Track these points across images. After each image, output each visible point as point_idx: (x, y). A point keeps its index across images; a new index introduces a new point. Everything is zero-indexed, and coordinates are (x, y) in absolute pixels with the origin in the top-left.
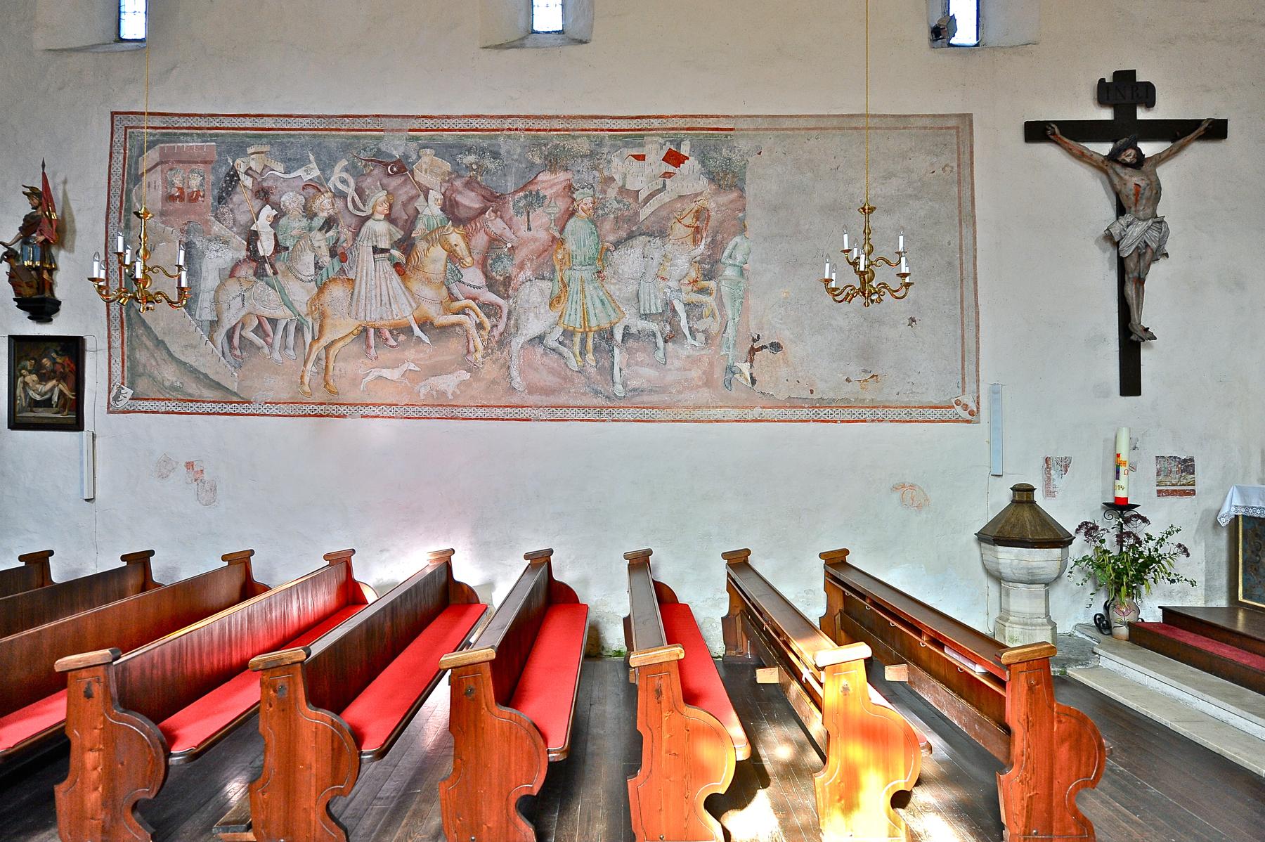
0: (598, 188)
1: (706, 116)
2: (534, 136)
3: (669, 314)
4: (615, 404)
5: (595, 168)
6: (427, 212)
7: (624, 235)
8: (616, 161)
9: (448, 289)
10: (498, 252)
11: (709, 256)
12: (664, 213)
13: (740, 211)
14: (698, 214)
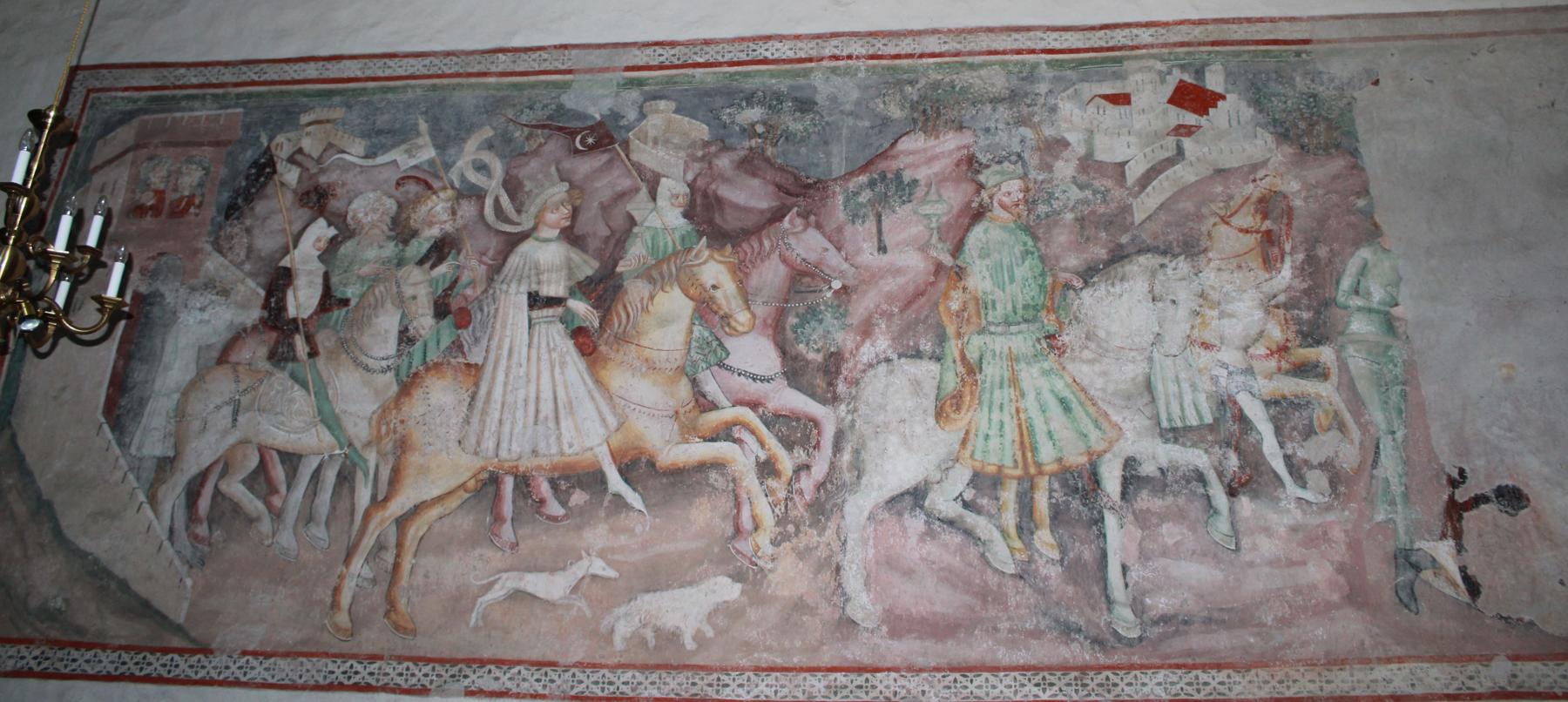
0: (1033, 160)
1: (1249, 20)
2: (888, 68)
3: (1229, 425)
4: (1116, 659)
5: (1022, 121)
6: (653, 221)
7: (1102, 253)
8: (1067, 107)
9: (694, 382)
10: (811, 299)
11: (1307, 292)
12: (1188, 205)
13: (1359, 195)
14: (1265, 205)
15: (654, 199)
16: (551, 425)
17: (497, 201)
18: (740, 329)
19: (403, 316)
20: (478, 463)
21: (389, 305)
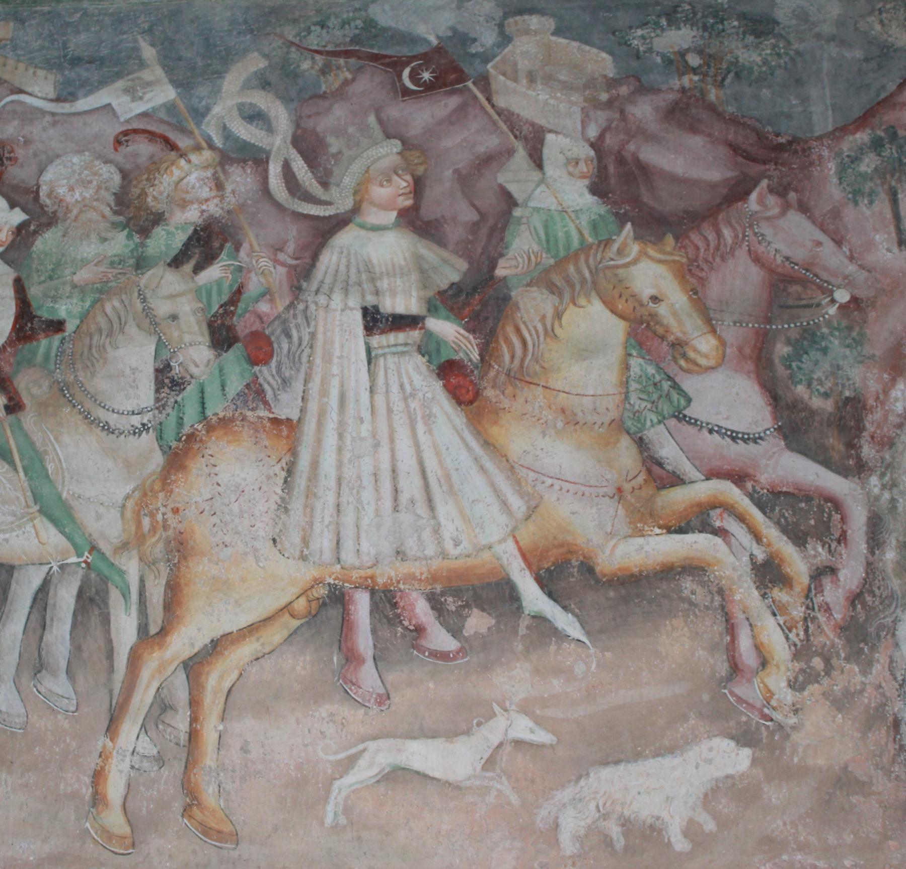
6: (543, 199)
9: (641, 443)
10: (805, 318)
15: (540, 166)
16: (422, 509)
17: (287, 167)
18: (703, 362)
19: (160, 345)
20: (306, 573)
21: (132, 329)
